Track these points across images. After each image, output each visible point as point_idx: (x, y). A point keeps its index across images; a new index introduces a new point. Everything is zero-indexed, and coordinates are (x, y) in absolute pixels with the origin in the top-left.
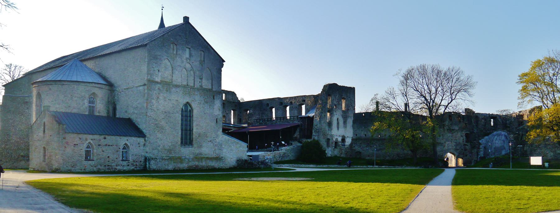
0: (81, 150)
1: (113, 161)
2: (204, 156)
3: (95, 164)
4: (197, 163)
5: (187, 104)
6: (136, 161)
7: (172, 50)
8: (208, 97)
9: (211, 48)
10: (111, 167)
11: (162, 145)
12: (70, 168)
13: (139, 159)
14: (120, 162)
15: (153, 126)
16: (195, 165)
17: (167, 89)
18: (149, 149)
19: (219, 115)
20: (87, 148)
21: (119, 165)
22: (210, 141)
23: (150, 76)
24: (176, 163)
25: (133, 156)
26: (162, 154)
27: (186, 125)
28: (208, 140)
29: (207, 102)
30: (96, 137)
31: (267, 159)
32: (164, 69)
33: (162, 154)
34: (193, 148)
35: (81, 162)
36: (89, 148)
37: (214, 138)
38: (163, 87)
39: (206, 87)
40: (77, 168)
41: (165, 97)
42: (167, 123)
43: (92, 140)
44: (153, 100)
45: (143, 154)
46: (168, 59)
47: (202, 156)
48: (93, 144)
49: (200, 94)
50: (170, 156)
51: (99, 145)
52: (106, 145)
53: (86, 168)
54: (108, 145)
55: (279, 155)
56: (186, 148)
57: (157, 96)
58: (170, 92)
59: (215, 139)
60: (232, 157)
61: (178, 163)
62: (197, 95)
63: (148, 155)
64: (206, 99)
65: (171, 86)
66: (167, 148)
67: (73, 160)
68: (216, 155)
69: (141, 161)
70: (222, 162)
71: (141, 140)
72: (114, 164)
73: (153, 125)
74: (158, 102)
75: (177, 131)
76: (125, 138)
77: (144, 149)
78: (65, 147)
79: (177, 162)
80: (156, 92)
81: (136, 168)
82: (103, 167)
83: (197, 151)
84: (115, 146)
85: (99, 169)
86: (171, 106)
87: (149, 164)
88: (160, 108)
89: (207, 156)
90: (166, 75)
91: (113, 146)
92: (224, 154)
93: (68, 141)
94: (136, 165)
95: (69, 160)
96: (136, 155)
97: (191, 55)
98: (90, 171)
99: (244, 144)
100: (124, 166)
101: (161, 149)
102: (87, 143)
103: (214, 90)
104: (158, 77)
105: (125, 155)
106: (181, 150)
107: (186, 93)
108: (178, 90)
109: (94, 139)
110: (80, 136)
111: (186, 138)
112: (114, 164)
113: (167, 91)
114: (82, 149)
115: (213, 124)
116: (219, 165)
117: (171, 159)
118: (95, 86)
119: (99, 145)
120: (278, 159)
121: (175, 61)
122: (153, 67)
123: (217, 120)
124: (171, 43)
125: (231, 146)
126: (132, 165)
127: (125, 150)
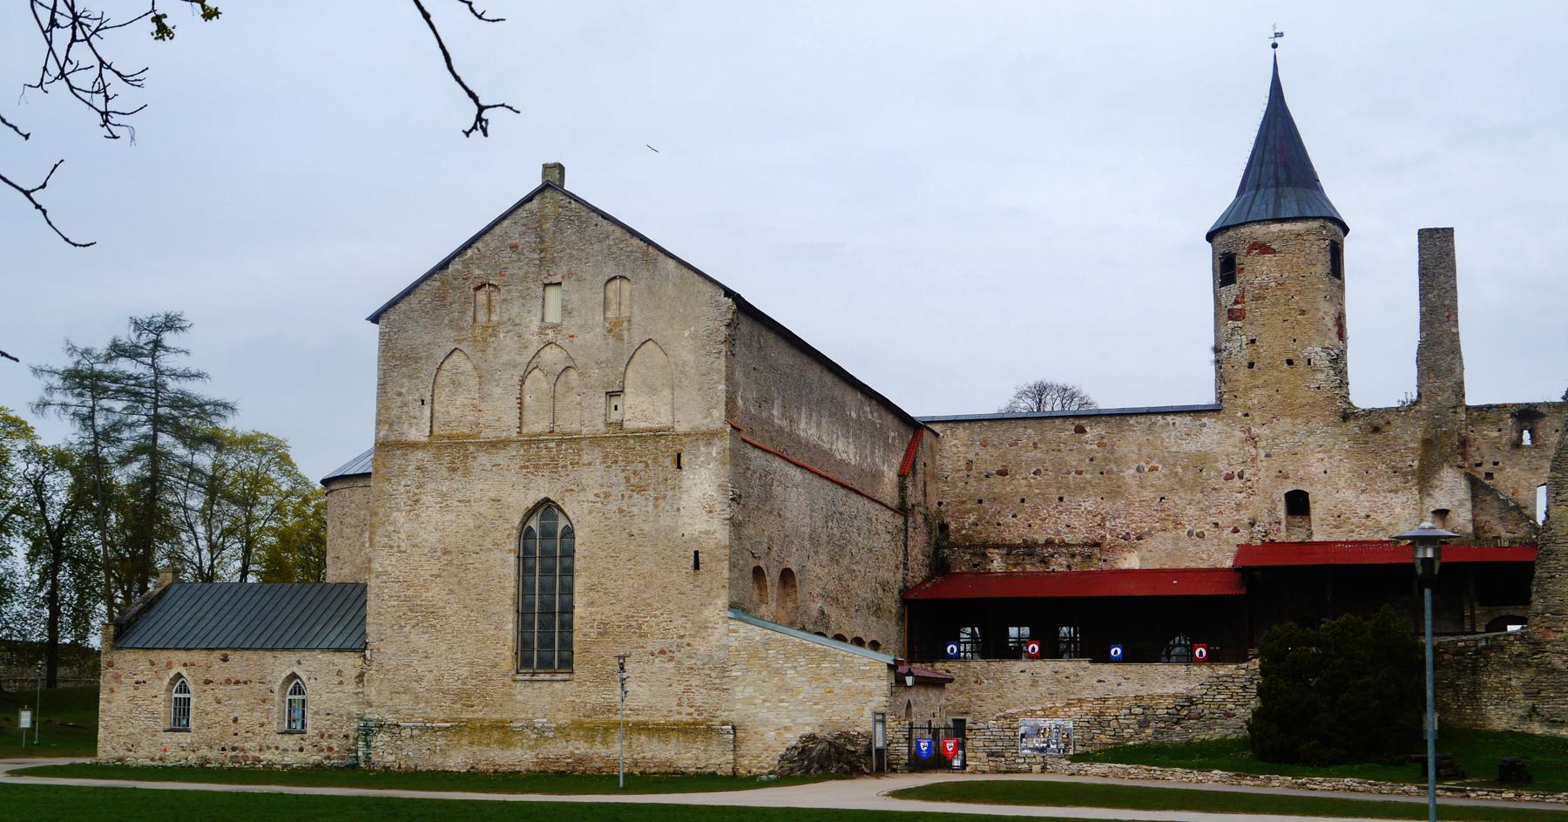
0: (154, 699)
1: (250, 734)
2: (627, 715)
3: (193, 744)
4: (580, 747)
5: (546, 507)
6: (330, 736)
7: (486, 311)
8: (647, 466)
9: (662, 256)
10: (242, 754)
11: (429, 677)
12: (121, 753)
13: (341, 727)
14: (272, 737)
15: (394, 607)
16: (572, 753)
17: (453, 463)
18: (379, 693)
19: (707, 533)
20: (180, 691)
21: (269, 748)
22: (662, 652)
23: (387, 427)
24: (480, 743)
25: (317, 717)
26: (428, 710)
27: (547, 590)
28: (649, 648)
29: (641, 489)
30: (196, 656)
31: (1038, 731)
32: (447, 390)
33: (428, 710)
34: (574, 684)
35: (155, 735)
36: (185, 692)
37: (682, 637)
38: (437, 457)
39: (643, 425)
40: (141, 753)
41: (445, 495)
42: (451, 591)
43: (185, 665)
44: (395, 514)
45: (354, 709)
46: (461, 350)
47: (618, 718)
48: (189, 678)
49: (606, 456)
50: (466, 716)
51: (207, 682)
52: (228, 681)
53: (167, 754)
54: (233, 681)
55: (1138, 710)
56: (537, 685)
57: (411, 494)
58: (467, 473)
59: (686, 640)
60: (787, 722)
61: (488, 745)
62: (590, 464)
63: (373, 715)
64: (635, 473)
65: (472, 449)
66: (455, 685)
67: (131, 729)
68: (690, 714)
69: (346, 737)
70: (720, 744)
71: (349, 663)
72: (253, 744)
73: (396, 603)
74: (418, 516)
75: (495, 618)
76: (294, 656)
77: (359, 692)
78: (112, 691)
79: (486, 741)
80: (409, 483)
81: (328, 758)
82: (216, 751)
83: (595, 698)
84: (259, 685)
85: (207, 760)
86: (471, 524)
87: (368, 746)
88: (425, 536)
89: (641, 718)
90: (455, 412)
91: (252, 685)
92: (739, 706)
93: (120, 672)
94: (330, 749)
95: (120, 728)
96: (328, 714)
97: (566, 311)
98: (177, 763)
99: (865, 660)
100: (285, 750)
101: (427, 690)
102: (171, 676)
104: (417, 424)
105: (297, 715)
106: (514, 692)
108: (501, 457)
109: (193, 665)
110: (153, 655)
111: (546, 644)
112: (253, 744)
113: (454, 470)
114: (156, 697)
115: (680, 574)
116: (702, 755)
117: (458, 729)
119: (207, 682)
120: (1127, 733)
121: (490, 350)
122: (400, 394)
124: (477, 289)
125: (778, 672)
126: (315, 749)
127: (301, 697)
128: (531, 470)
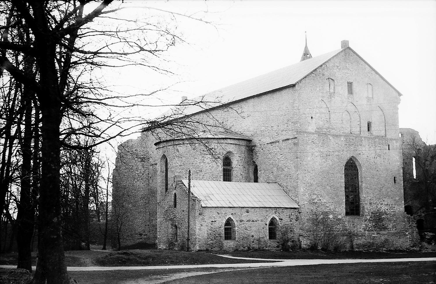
43: (232, 214)
52: (249, 221)
103: (388, 137)
107: (349, 145)
118: (230, 142)
123: (395, 179)
128: (348, 146)
